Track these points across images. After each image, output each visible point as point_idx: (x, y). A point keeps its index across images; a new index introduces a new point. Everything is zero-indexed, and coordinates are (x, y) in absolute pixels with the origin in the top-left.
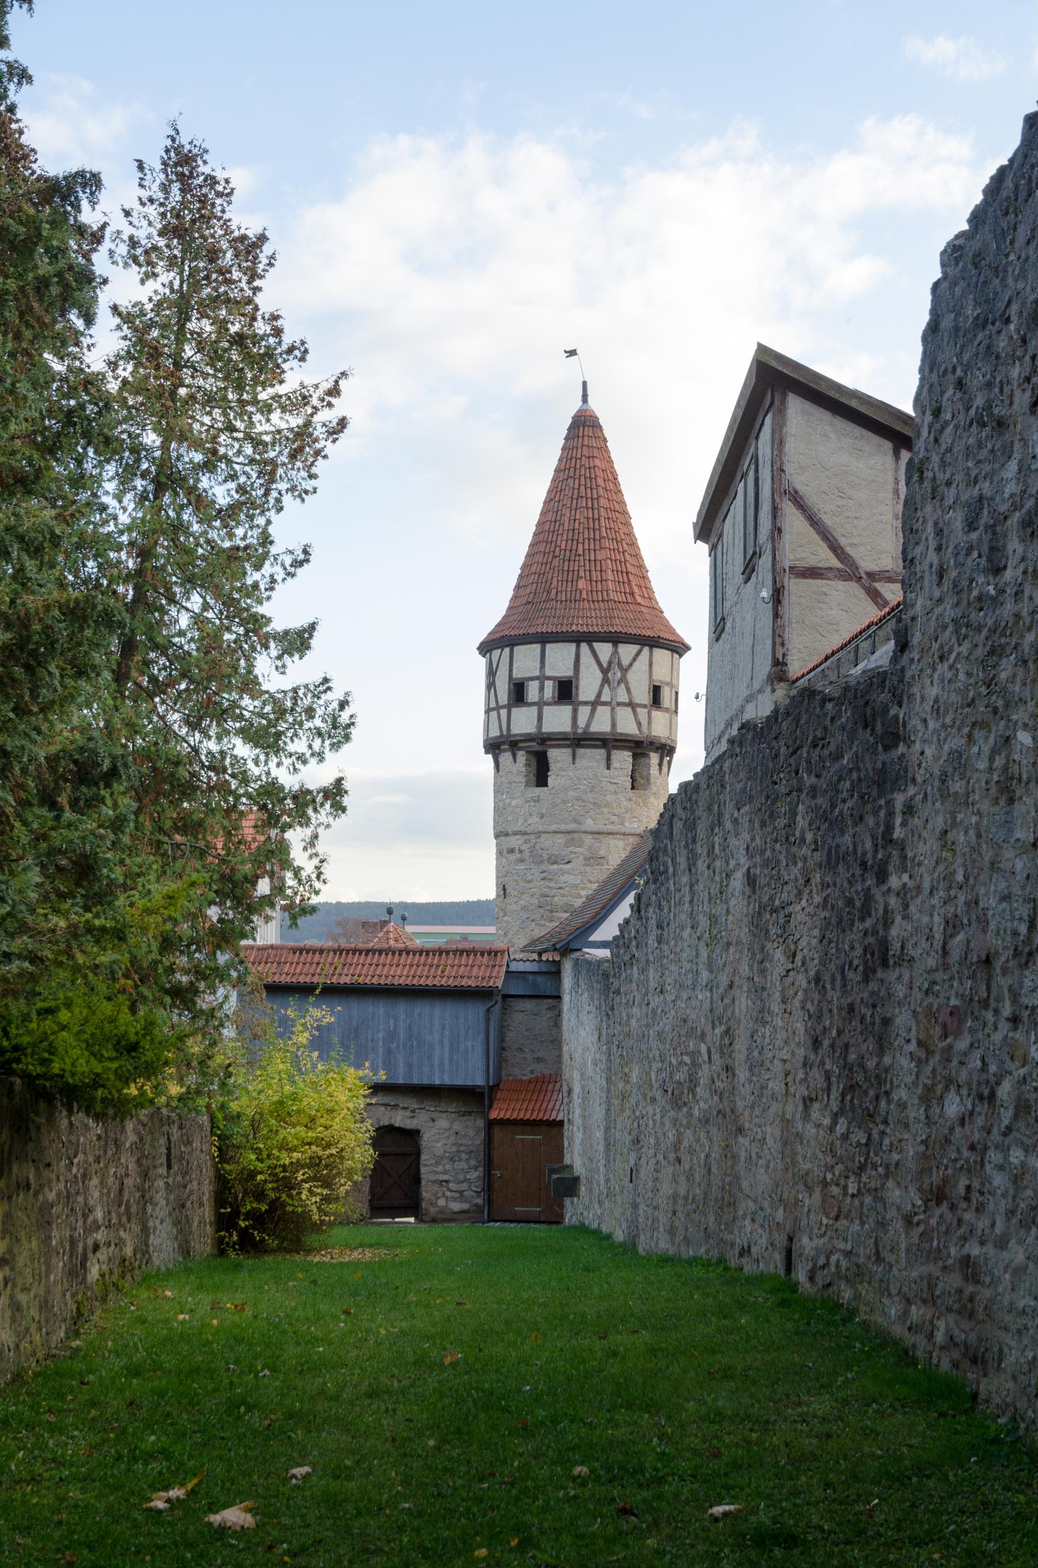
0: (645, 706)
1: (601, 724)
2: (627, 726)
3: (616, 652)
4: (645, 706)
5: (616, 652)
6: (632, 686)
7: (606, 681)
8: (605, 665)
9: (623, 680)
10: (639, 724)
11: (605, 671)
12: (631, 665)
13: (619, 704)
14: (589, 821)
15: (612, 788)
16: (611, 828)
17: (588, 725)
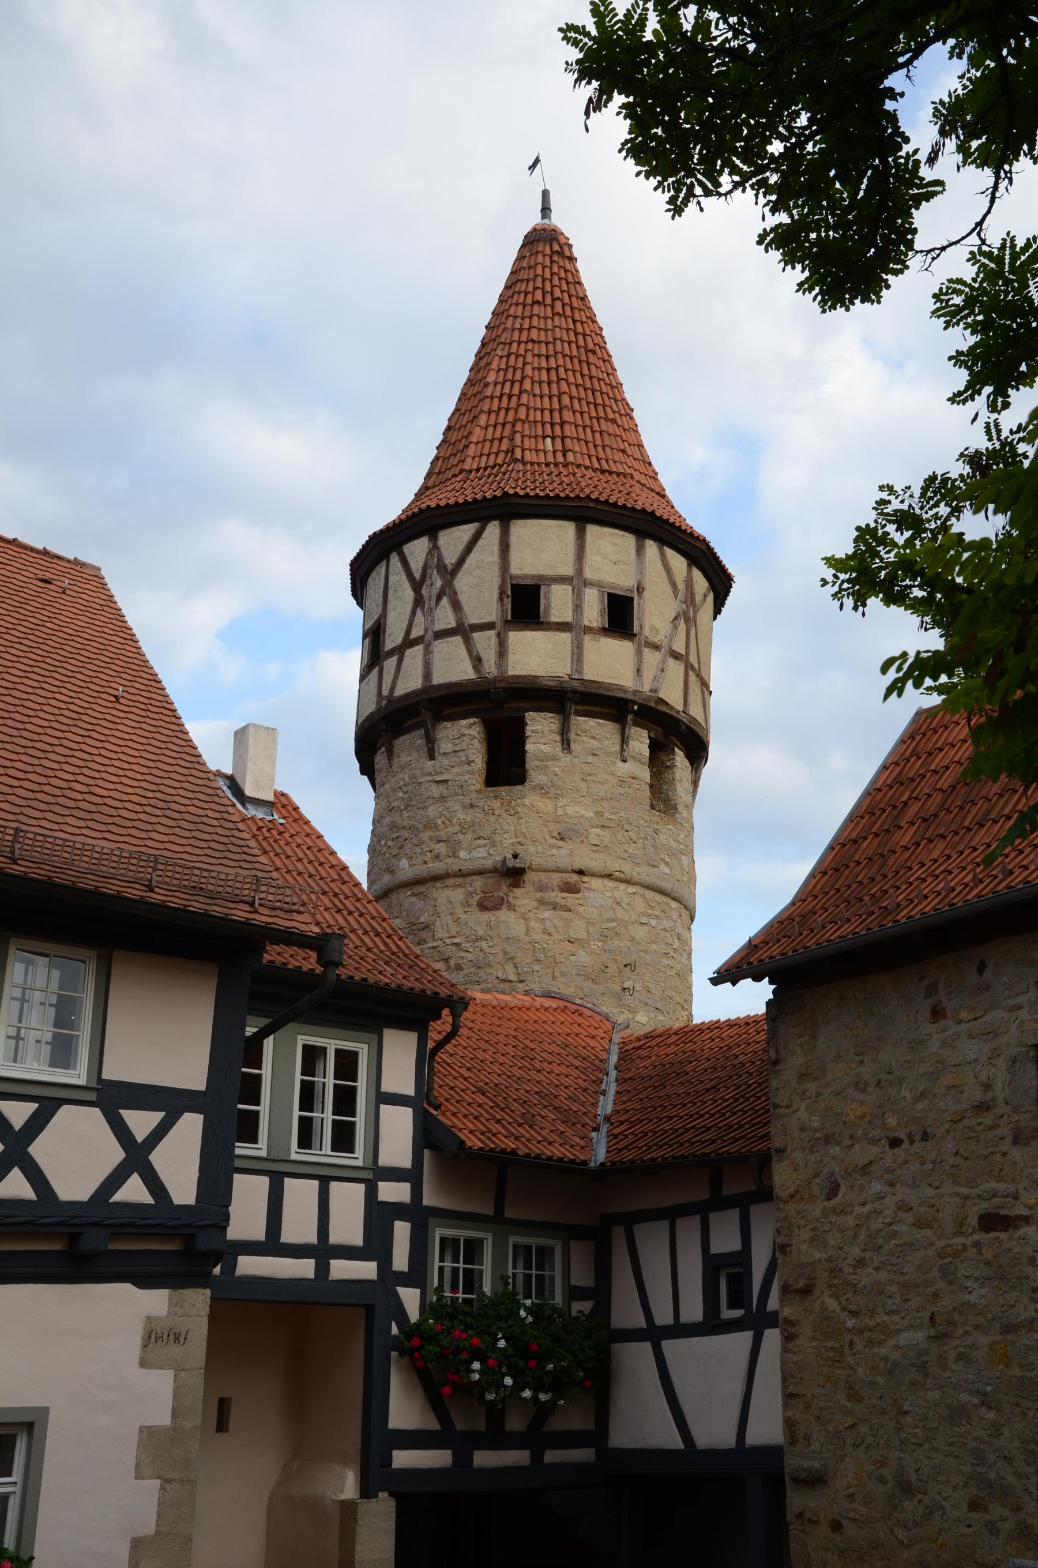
0: (490, 626)
1: (411, 681)
2: (453, 665)
4: (490, 626)
5: (435, 547)
6: (463, 598)
7: (419, 602)
8: (417, 576)
9: (448, 591)
10: (477, 661)
11: (417, 586)
12: (461, 561)
14: (404, 863)
15: (436, 791)
16: (437, 867)
17: (392, 689)
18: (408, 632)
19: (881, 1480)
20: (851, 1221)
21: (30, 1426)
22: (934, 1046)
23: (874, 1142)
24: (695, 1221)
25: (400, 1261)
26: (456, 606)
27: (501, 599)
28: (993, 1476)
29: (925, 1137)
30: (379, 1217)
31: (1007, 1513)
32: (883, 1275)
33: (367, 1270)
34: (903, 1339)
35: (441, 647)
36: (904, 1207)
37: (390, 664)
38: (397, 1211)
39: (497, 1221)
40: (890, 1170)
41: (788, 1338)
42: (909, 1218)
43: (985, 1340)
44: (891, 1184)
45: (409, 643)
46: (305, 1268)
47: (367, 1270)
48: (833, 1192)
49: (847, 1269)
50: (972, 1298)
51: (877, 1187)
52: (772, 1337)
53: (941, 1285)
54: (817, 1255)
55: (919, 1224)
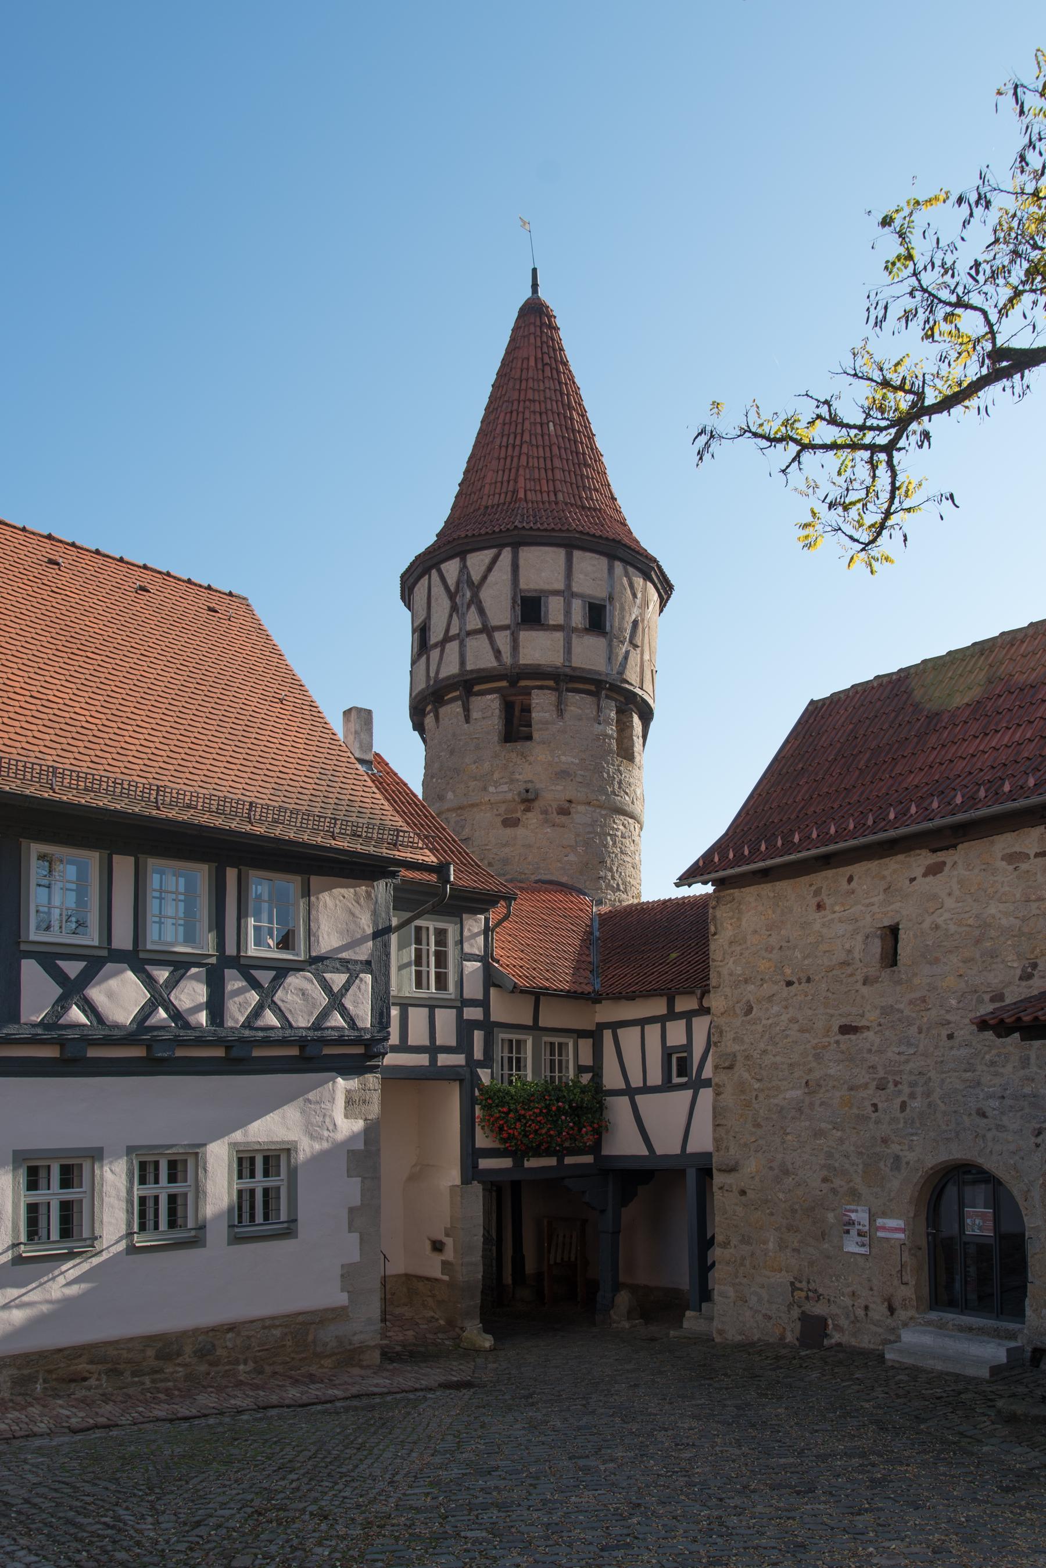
2: (480, 656)
3: (464, 568)
7: (454, 608)
10: (497, 653)
13: (469, 634)
18: (447, 630)
19: (771, 1168)
20: (760, 1028)
21: (289, 1150)
22: (817, 926)
23: (776, 983)
24: (658, 1026)
25: (478, 1054)
26: (481, 612)
27: (513, 607)
28: (837, 1165)
29: (809, 980)
30: (465, 1029)
31: (843, 1183)
32: (778, 1059)
33: (459, 1059)
34: (789, 1095)
35: (471, 643)
36: (793, 1020)
37: (435, 654)
38: (475, 1024)
39: (535, 1028)
40: (786, 999)
41: (718, 1094)
42: (796, 1027)
43: (838, 1094)
44: (786, 1007)
45: (447, 639)
46: (423, 1059)
47: (459, 1059)
48: (749, 1010)
49: (756, 1055)
50: (832, 1072)
51: (776, 1009)
52: (706, 1095)
53: (814, 1064)
54: (737, 1047)
55: (802, 1031)
